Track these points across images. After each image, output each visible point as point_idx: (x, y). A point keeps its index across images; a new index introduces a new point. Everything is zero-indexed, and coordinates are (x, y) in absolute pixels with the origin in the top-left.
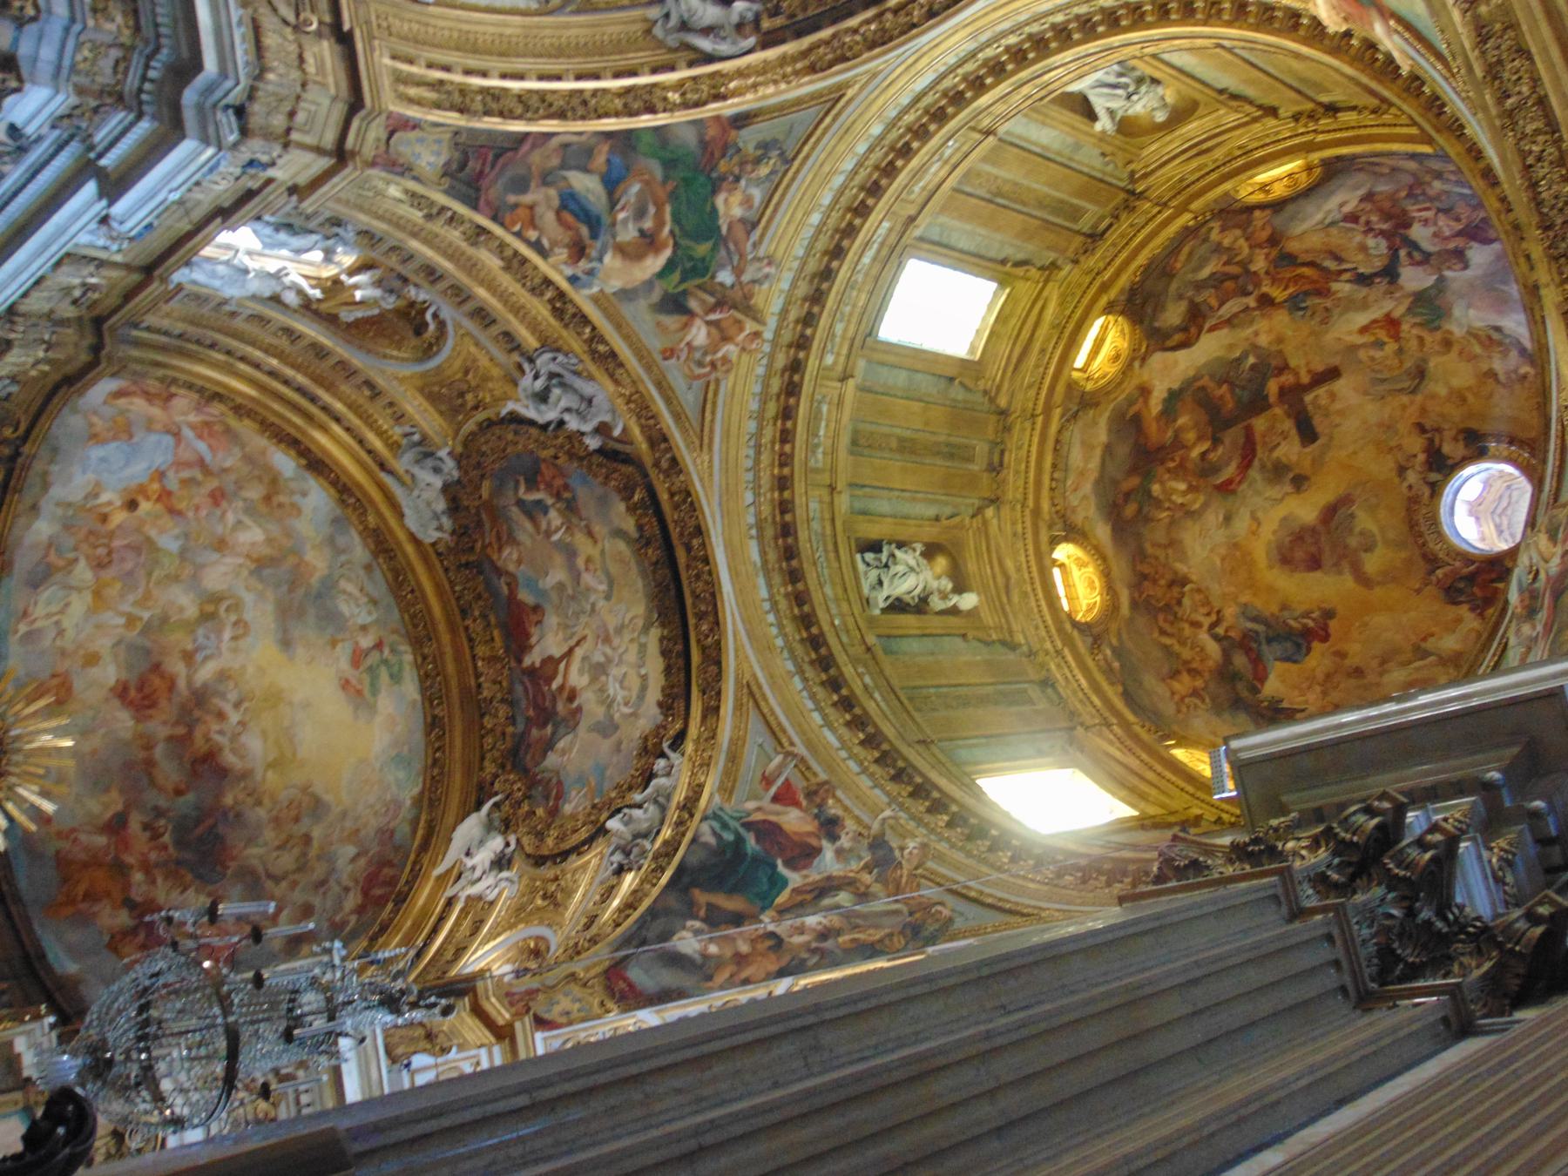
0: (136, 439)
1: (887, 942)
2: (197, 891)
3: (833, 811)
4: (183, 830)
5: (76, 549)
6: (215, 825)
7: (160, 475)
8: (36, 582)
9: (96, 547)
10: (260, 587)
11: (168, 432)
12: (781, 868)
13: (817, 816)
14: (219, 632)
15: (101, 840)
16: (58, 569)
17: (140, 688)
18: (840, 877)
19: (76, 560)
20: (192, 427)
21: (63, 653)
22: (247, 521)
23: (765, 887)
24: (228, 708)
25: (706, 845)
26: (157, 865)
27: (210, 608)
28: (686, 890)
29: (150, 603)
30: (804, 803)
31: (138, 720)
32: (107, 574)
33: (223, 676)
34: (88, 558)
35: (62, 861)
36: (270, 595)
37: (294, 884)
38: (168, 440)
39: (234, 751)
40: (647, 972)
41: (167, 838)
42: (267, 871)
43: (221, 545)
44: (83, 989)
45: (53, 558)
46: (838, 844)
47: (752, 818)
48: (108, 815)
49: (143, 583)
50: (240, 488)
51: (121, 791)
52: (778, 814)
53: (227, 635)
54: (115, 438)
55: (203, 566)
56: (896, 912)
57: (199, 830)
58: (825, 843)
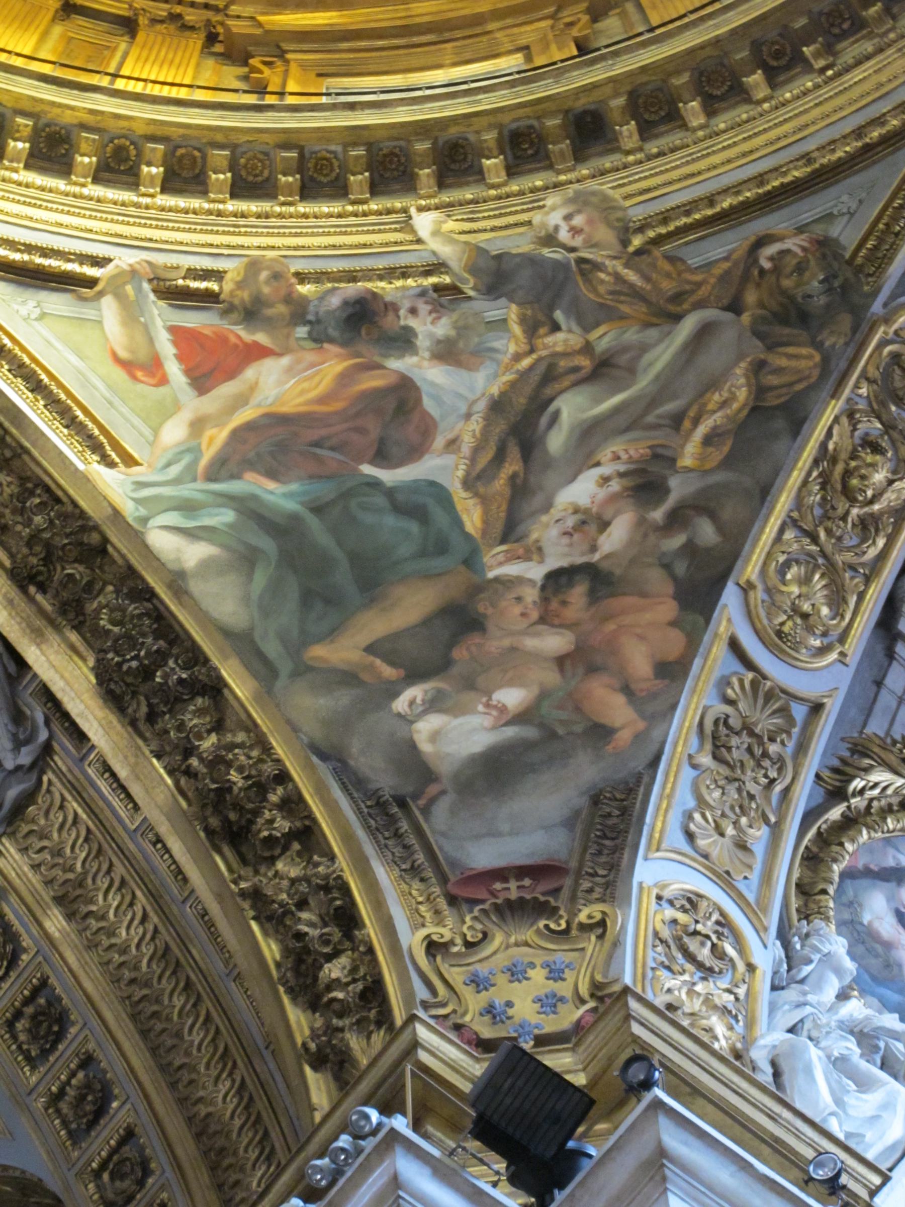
1: (773, 380)
3: (335, 301)
12: (388, 476)
13: (318, 338)
18: (513, 384)
23: (414, 527)
25: (206, 565)
28: (302, 670)
30: (261, 338)
40: (494, 834)
46: (423, 342)
47: (207, 456)
52: (241, 401)
56: (704, 332)
58: (398, 364)
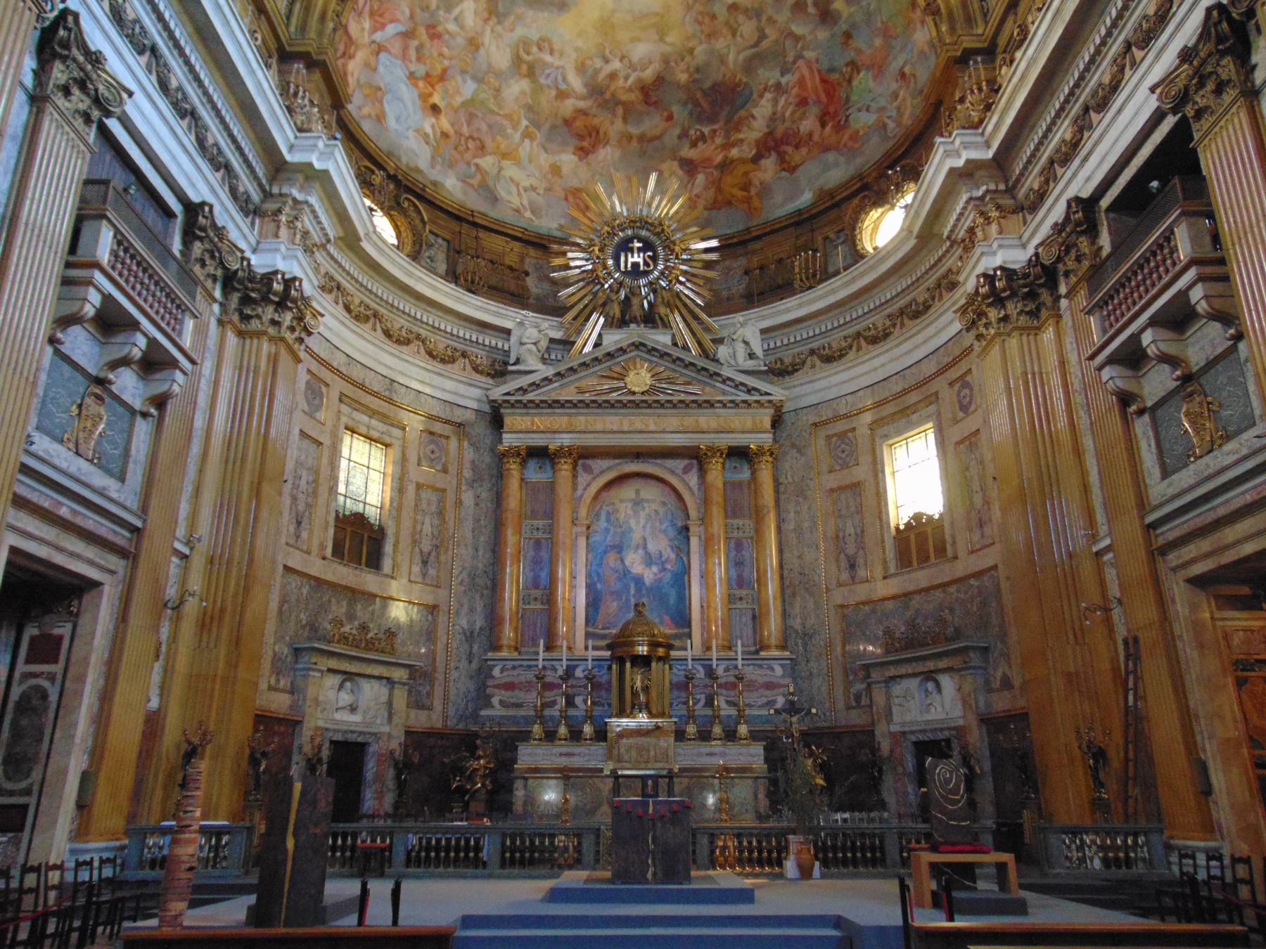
0: (382, 85)
2: (756, 106)
4: (702, 116)
5: (468, 164)
6: (702, 90)
7: (412, 76)
8: (494, 199)
9: (468, 148)
10: (512, 18)
11: (378, 54)
14: (546, 65)
15: (700, 178)
16: (484, 180)
17: (581, 137)
19: (477, 165)
20: (374, 30)
21: (548, 190)
22: (456, 11)
24: (608, 69)
26: (727, 136)
27: (524, 67)
29: (515, 117)
31: (607, 142)
32: (490, 145)
33: (581, 68)
34: (475, 157)
35: (714, 206)
36: (520, 10)
37: (771, 21)
38: (383, 56)
39: (643, 70)
41: (706, 130)
42: (752, 47)
43: (474, 44)
44: (826, 188)
45: (475, 182)
48: (680, 172)
49: (498, 118)
50: (428, 7)
51: (663, 161)
53: (548, 58)
54: (381, 103)
55: (490, 64)
57: (705, 105)
